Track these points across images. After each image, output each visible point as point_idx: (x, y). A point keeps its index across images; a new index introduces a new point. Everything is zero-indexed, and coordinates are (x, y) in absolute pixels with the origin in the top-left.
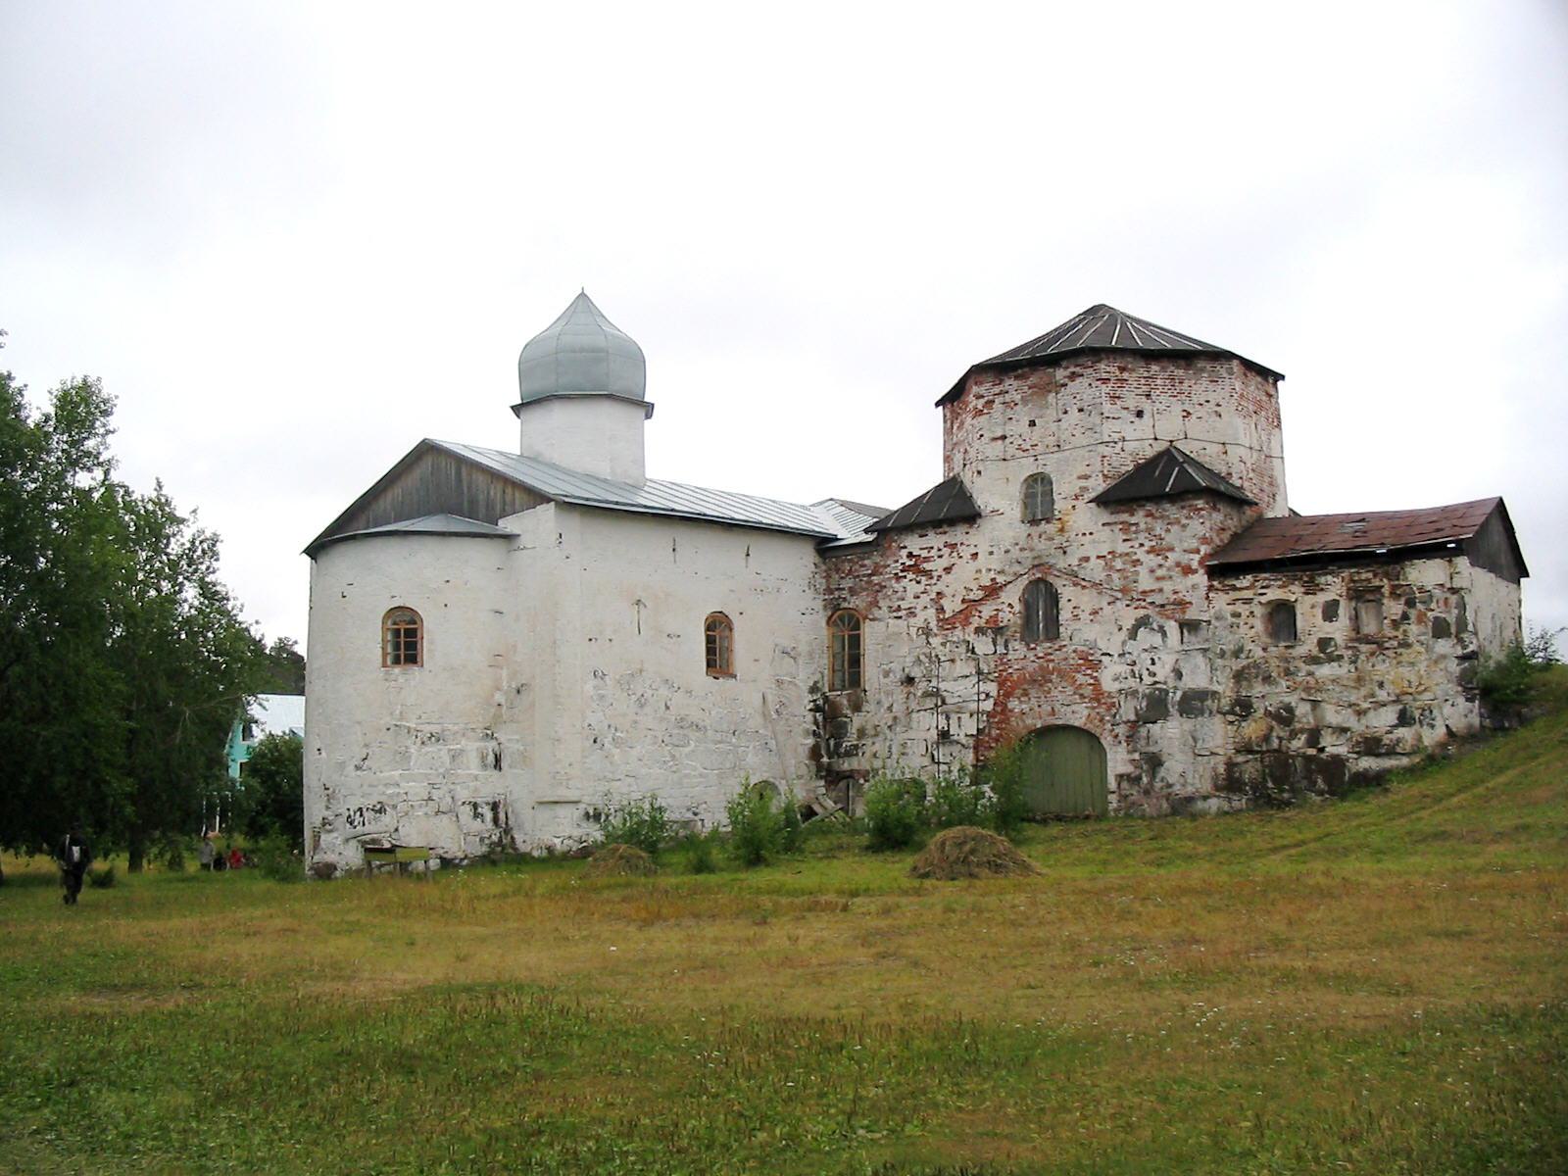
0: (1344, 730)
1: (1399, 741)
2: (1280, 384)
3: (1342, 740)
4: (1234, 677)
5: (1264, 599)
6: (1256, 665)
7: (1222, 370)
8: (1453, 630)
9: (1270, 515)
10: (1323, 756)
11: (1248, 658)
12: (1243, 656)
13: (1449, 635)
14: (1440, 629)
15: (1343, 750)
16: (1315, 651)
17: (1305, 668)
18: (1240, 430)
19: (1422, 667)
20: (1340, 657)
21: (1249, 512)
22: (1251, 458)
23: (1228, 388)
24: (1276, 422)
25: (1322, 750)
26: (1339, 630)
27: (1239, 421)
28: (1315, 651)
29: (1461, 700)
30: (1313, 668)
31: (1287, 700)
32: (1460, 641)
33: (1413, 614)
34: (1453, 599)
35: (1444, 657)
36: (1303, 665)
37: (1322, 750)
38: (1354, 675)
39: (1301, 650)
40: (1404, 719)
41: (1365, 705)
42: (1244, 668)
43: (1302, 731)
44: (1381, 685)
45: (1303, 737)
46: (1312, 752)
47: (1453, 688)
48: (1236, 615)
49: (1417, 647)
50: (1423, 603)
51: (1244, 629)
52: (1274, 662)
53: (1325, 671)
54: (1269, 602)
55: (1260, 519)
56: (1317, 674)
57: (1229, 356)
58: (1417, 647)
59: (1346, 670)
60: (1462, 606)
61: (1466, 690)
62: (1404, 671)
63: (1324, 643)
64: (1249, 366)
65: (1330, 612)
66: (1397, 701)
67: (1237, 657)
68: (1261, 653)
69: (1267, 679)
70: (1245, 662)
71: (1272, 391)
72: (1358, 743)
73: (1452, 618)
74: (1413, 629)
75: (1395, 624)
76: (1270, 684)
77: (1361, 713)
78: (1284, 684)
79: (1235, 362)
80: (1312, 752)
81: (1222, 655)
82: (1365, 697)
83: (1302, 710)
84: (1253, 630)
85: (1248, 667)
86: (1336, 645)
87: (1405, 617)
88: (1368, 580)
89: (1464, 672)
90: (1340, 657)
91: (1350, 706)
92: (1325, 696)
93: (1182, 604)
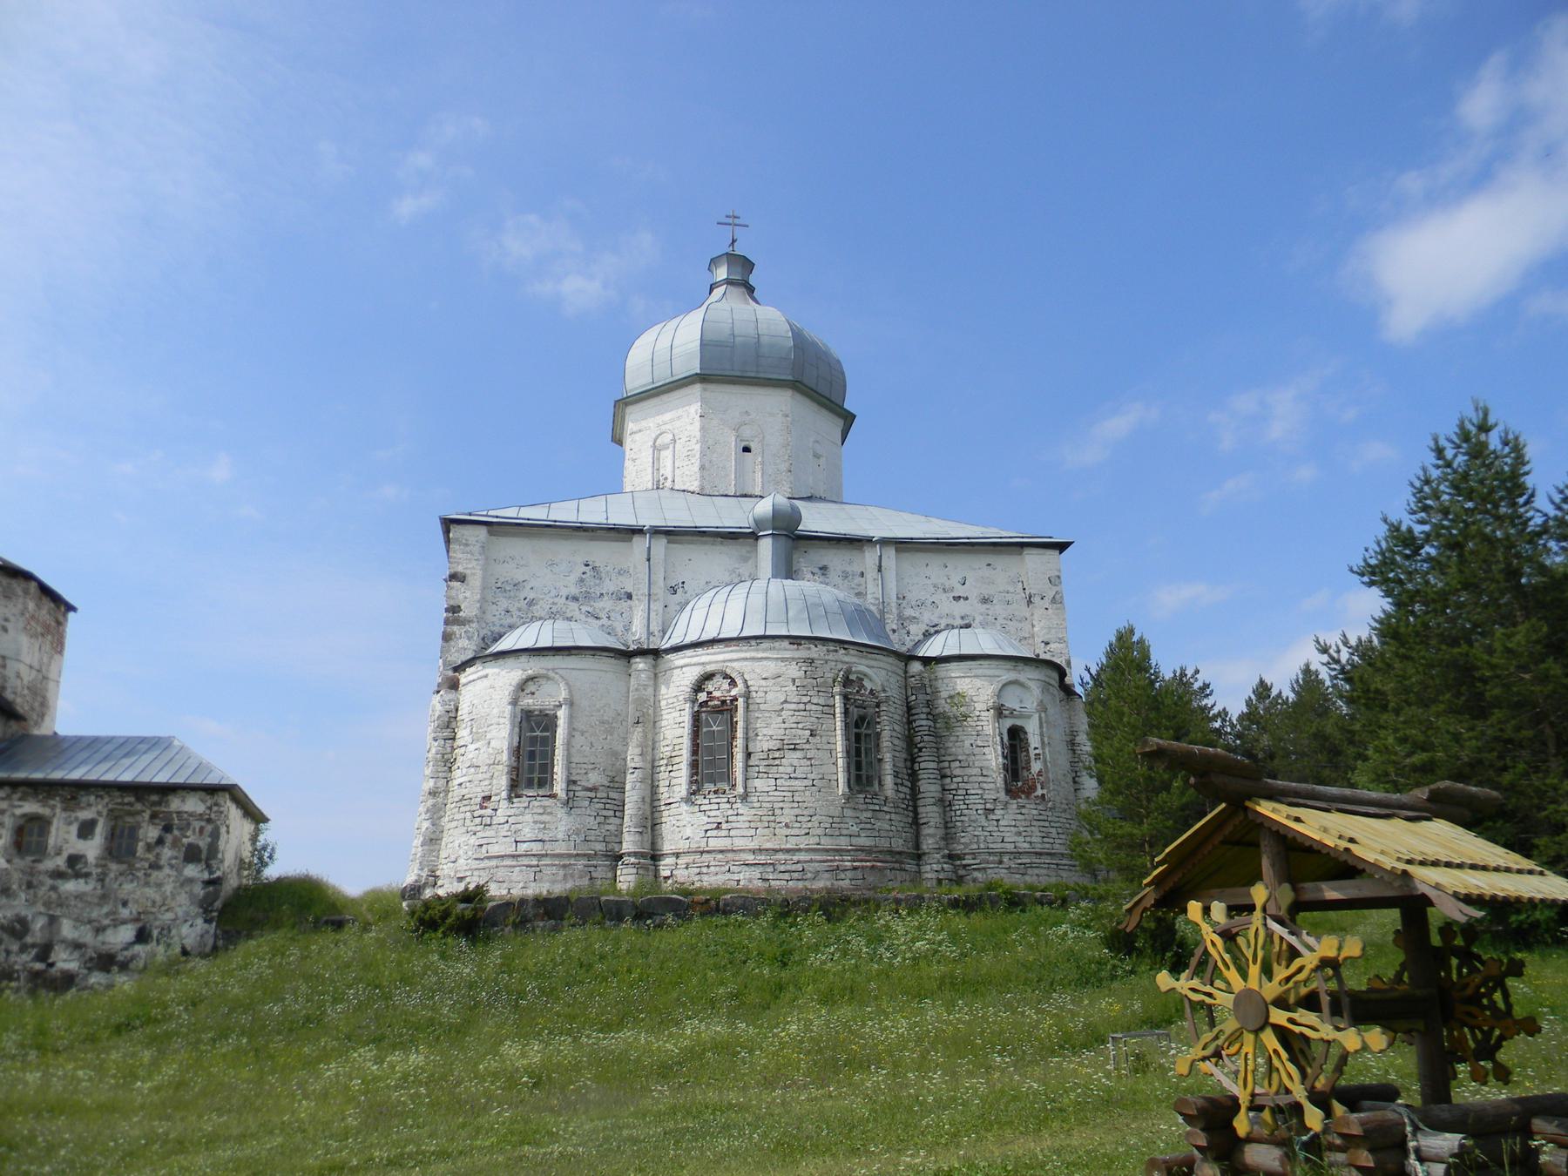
0: (77, 946)
1: (133, 958)
2: (71, 615)
3: (76, 954)
5: (18, 812)
7: (17, 586)
8: (204, 856)
9: (36, 732)
10: (53, 971)
13: (199, 860)
14: (192, 855)
15: (73, 966)
17: (49, 882)
18: (25, 650)
19: (168, 888)
20: (87, 875)
21: (14, 726)
22: (28, 676)
23: (20, 606)
24: (59, 646)
25: (52, 965)
26: (92, 849)
27: (24, 640)
29: (200, 921)
30: (59, 882)
31: (23, 913)
32: (208, 866)
33: (169, 838)
34: (209, 828)
35: (191, 881)
37: (52, 965)
38: (99, 892)
39: (49, 864)
40: (142, 936)
41: (106, 922)
43: (33, 946)
44: (125, 904)
45: (34, 952)
46: (39, 966)
47: (195, 910)
49: (167, 870)
50: (180, 829)
52: (16, 876)
53: (70, 886)
54: (24, 815)
55: (26, 737)
57: (27, 576)
58: (167, 870)
60: (215, 835)
61: (206, 911)
62: (151, 892)
63: (74, 860)
64: (46, 591)
65: (86, 830)
66: (137, 920)
71: (61, 619)
72: (91, 959)
73: (203, 843)
74: (167, 853)
75: (149, 848)
77: (99, 930)
78: (23, 896)
79: (33, 584)
80: (39, 966)
82: (107, 915)
83: (39, 924)
87: (160, 841)
88: (131, 804)
89: (207, 895)
90: (87, 875)
91: (90, 922)
92: (65, 910)
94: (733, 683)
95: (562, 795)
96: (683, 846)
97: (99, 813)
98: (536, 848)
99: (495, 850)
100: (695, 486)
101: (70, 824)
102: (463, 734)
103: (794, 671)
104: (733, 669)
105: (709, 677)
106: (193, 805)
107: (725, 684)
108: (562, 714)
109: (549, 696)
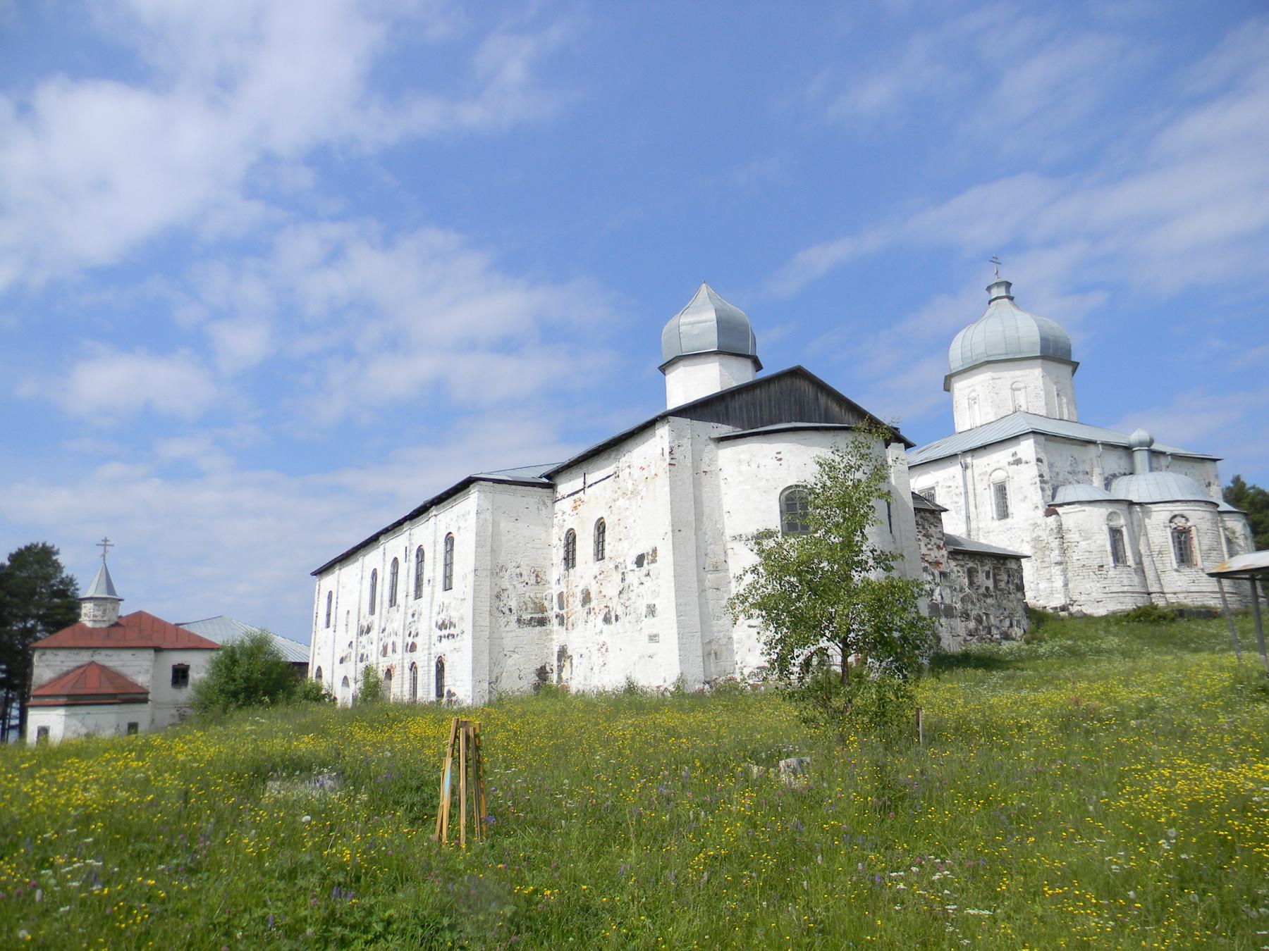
93: (938, 563)
94: (1187, 520)
95: (1134, 566)
96: (1179, 589)
98: (1130, 589)
99: (1114, 589)
100: (1043, 413)
102: (1072, 536)
103: (1208, 516)
104: (1186, 513)
105: (1175, 517)
106: (1013, 565)
107: (1183, 520)
108: (1124, 530)
109: (1121, 522)
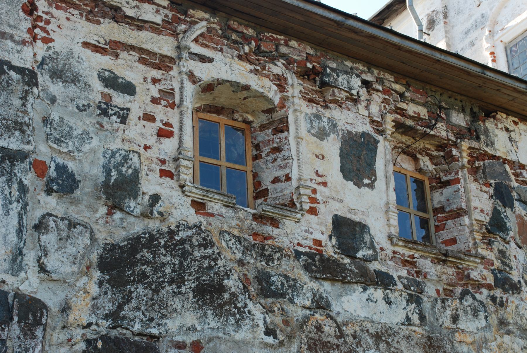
4: (104, 265)
6: (174, 242)
11: (146, 215)
12: (135, 206)
16: (330, 249)
20: (384, 281)
26: (376, 207)
28: (330, 249)
30: (327, 288)
36: (304, 277)
42: (135, 243)
48: (111, 81)
51: (139, 132)
56: (336, 307)
59: (400, 317)
63: (348, 231)
67: (115, 206)
68: (192, 217)
69: (210, 293)
70: (138, 227)
76: (220, 311)
78: (256, 310)
81: (64, 183)
84: (157, 142)
85: (150, 241)
86: (372, 246)
97: (377, 125)
101: (322, 135)
